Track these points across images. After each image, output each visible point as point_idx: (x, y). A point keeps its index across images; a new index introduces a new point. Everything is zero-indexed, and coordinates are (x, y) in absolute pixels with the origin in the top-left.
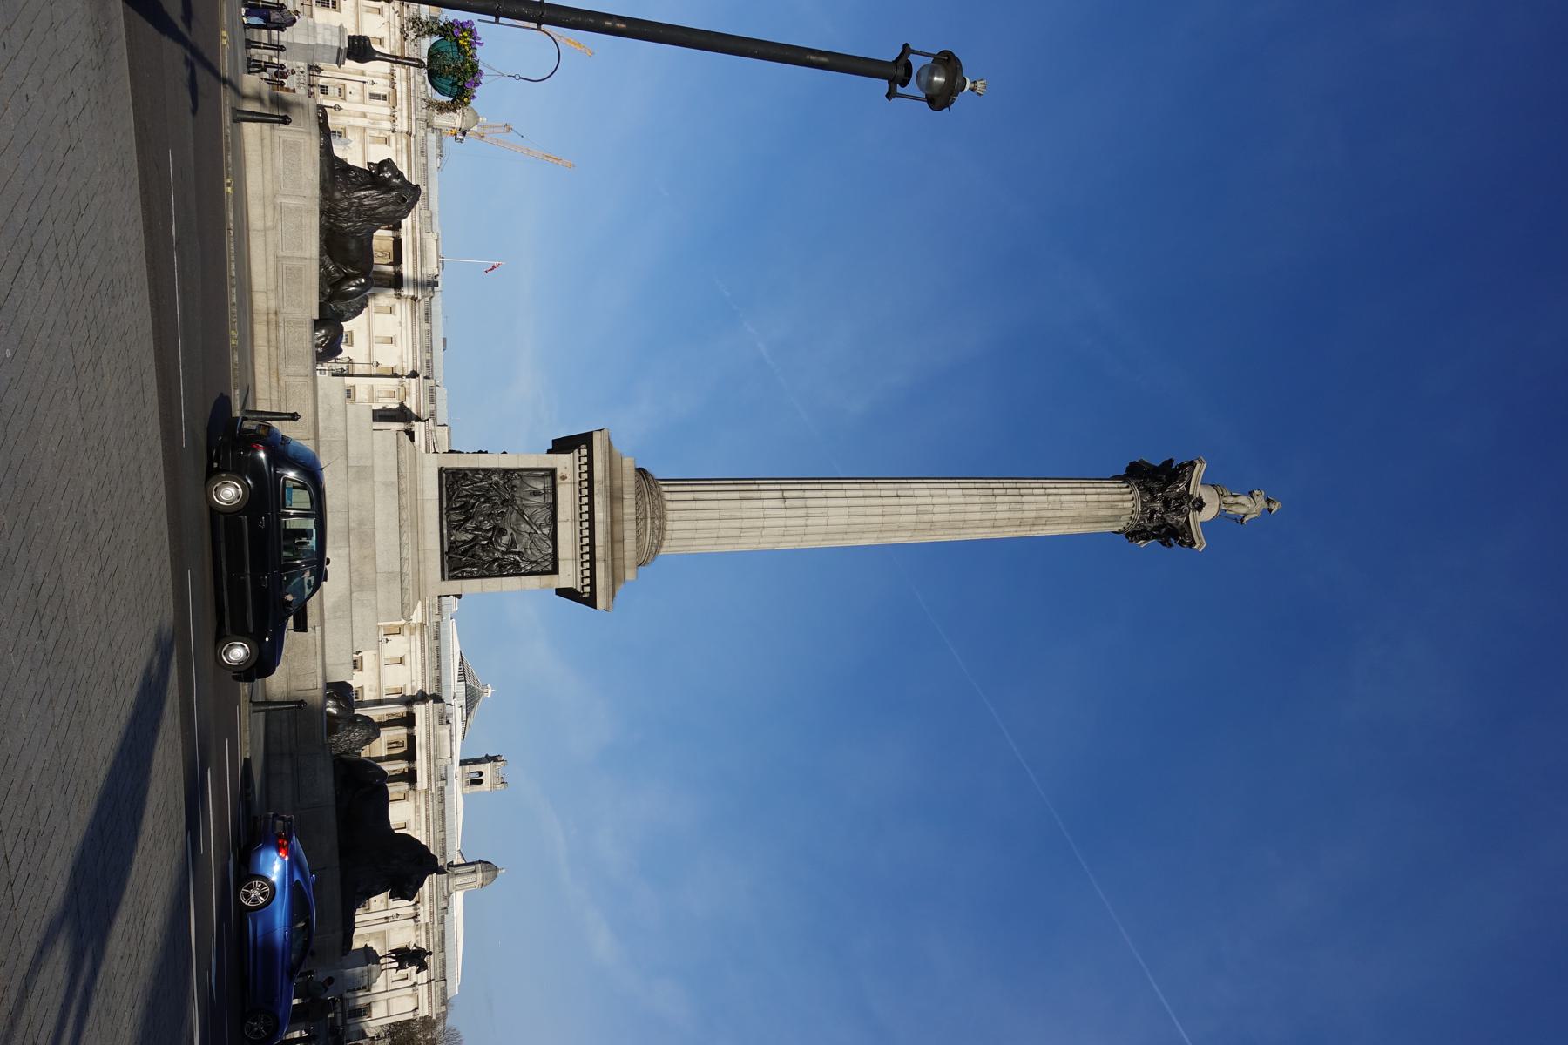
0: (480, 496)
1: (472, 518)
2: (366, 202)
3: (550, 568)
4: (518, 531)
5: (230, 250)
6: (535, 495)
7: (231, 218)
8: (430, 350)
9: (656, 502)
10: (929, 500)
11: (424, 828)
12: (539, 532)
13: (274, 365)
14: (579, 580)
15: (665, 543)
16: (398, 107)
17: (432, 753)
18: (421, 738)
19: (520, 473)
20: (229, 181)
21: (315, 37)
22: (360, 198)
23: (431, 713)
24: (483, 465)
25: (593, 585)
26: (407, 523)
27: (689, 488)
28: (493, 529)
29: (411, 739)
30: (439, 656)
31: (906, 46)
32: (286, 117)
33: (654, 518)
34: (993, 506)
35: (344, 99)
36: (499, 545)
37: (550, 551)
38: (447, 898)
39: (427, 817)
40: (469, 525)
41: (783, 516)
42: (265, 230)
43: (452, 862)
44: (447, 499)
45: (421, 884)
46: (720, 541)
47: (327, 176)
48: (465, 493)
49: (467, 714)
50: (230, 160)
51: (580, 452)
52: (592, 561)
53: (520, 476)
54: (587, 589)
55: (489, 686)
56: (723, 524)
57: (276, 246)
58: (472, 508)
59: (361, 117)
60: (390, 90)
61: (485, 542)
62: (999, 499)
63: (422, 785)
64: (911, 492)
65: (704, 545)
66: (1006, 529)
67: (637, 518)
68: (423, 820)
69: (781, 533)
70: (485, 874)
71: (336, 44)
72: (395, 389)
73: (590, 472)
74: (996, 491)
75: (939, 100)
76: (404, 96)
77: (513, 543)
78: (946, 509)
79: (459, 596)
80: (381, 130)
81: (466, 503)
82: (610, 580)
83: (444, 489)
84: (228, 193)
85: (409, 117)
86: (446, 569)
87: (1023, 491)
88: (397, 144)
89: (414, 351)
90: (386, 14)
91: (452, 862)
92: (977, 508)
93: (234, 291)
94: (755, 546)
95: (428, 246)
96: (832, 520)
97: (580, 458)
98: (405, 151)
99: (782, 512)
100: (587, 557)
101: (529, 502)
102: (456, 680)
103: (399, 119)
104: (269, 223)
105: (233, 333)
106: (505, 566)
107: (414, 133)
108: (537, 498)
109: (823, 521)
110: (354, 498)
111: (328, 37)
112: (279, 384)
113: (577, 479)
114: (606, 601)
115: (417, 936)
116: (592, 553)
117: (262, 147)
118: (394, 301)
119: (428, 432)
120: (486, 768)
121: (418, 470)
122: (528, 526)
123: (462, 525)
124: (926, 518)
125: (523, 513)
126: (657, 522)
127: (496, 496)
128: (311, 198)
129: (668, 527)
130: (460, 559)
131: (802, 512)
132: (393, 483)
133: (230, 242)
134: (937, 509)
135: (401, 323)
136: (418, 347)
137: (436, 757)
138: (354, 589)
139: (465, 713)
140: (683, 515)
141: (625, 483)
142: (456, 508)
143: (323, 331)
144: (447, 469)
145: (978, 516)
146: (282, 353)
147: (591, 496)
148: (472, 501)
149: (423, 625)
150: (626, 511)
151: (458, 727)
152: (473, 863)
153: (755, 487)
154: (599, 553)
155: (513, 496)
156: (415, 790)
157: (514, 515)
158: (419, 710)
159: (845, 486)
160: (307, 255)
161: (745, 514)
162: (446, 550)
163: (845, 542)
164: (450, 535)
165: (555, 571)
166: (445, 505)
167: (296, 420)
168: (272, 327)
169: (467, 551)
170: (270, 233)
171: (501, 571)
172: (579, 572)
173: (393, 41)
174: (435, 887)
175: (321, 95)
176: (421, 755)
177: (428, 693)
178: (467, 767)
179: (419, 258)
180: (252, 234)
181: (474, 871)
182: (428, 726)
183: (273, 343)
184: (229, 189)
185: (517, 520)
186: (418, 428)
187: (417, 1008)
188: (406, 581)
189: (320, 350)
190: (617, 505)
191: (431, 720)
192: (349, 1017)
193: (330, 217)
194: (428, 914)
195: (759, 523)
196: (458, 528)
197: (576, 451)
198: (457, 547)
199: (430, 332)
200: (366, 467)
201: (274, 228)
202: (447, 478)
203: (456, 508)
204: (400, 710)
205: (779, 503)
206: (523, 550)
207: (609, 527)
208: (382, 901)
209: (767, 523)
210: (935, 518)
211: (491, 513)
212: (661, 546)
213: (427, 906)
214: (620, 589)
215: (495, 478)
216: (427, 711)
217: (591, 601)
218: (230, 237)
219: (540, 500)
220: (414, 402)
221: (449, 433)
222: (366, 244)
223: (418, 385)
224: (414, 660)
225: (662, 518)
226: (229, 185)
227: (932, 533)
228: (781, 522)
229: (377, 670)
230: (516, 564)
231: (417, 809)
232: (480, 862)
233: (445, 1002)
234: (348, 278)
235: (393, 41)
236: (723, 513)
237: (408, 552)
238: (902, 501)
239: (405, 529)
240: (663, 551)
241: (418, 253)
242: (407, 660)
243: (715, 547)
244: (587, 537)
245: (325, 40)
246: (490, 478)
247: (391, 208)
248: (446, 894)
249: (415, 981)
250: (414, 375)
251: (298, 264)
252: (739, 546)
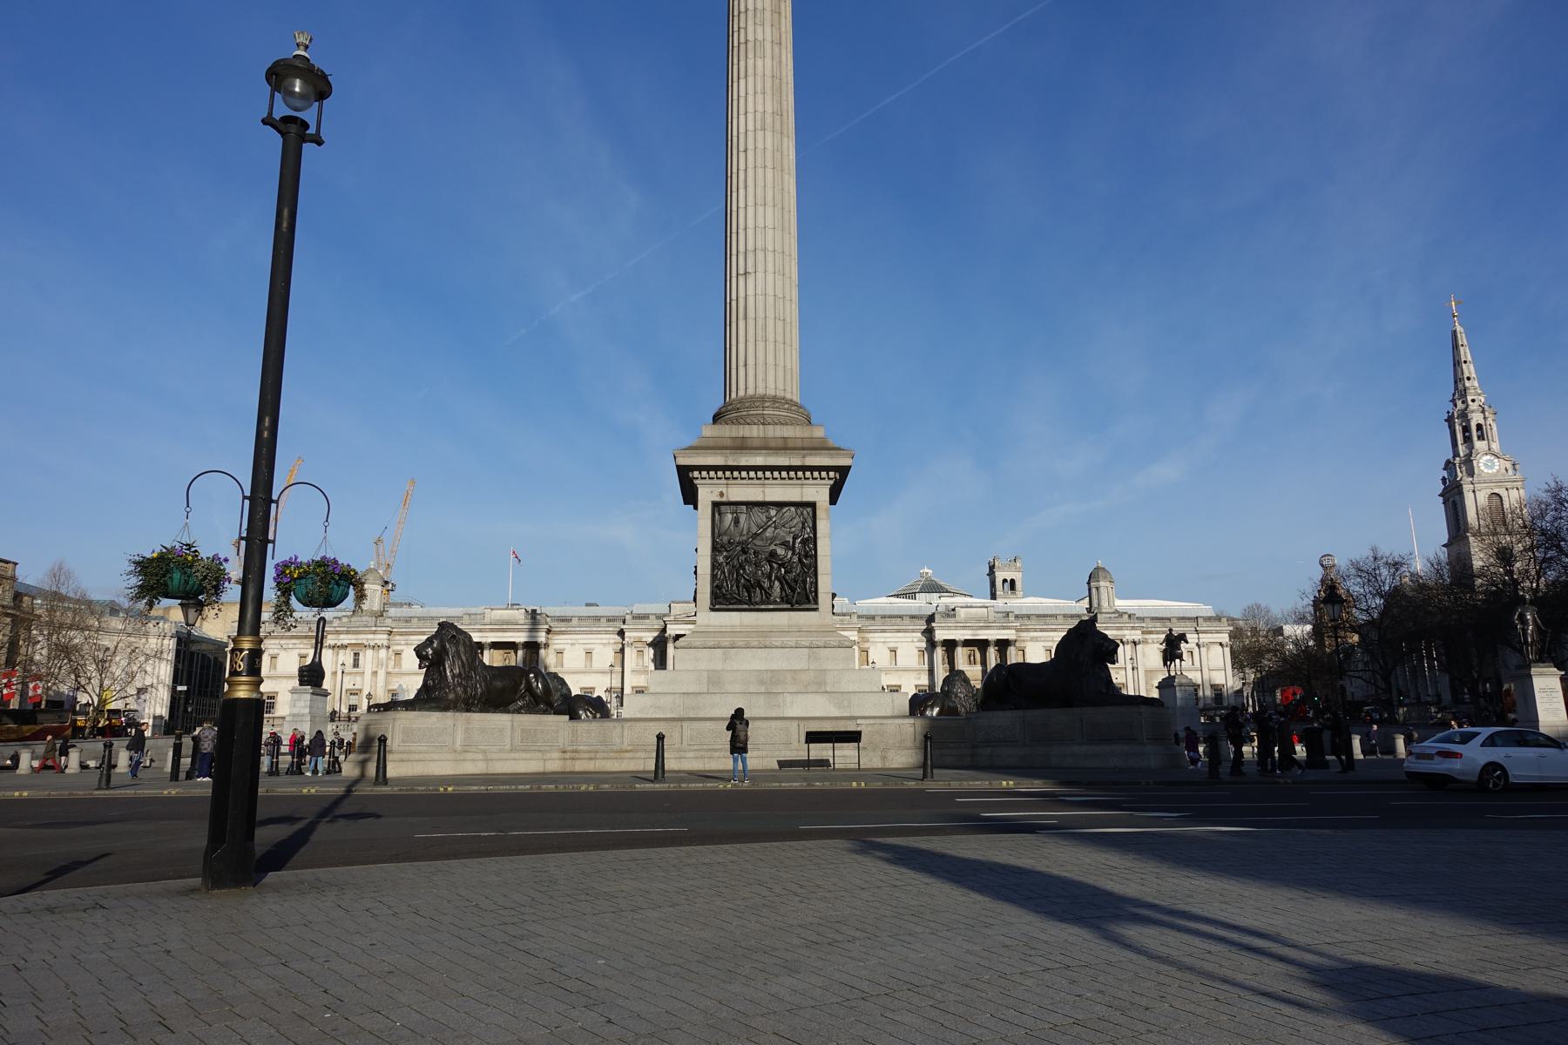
0: (738, 574)
1: (759, 582)
2: (457, 671)
3: (809, 509)
4: (773, 539)
5: (506, 789)
6: (738, 522)
7: (475, 788)
8: (597, 619)
9: (747, 405)
10: (750, 116)
11: (1052, 634)
12: (774, 519)
13: (612, 755)
14: (823, 482)
15: (788, 396)
16: (364, 642)
17: (982, 625)
18: (967, 635)
19: (716, 535)
20: (442, 789)
21: (303, 715)
22: (454, 676)
23: (943, 625)
24: (708, 571)
25: (828, 469)
26: (763, 641)
27: (734, 371)
28: (770, 562)
29: (967, 643)
30: (890, 617)
31: (264, 122)
32: (379, 739)
33: (763, 407)
34: (758, 44)
35: (360, 690)
36: (786, 557)
37: (793, 509)
38: (1121, 614)
39: (1042, 630)
40: (766, 585)
41: (763, 189)
42: (486, 760)
43: (1087, 609)
44: (741, 604)
45: (1106, 635)
46: (788, 341)
47: (433, 705)
48: (735, 588)
49: (947, 592)
50: (423, 788)
51: (697, 478)
52: (804, 468)
53: (719, 536)
54: (832, 474)
55: (921, 571)
56: (771, 337)
57: (501, 751)
58: (749, 581)
59: (376, 676)
60: (349, 649)
61: (783, 570)
62: (750, 37)
64: (742, 136)
65: (792, 358)
66: (783, 29)
67: (763, 424)
69: (781, 277)
70: (1101, 578)
71: (308, 697)
72: (635, 651)
73: (716, 468)
74: (742, 40)
75: (320, 88)
77: (785, 544)
78: (760, 96)
79: (834, 595)
80: (388, 659)
81: (744, 586)
82: (823, 452)
83: (731, 607)
84: (453, 790)
85: (374, 633)
86: (808, 606)
87: (742, 9)
88: (400, 644)
89: (599, 632)
90: (276, 651)
91: (1087, 609)
92: (759, 62)
93: (544, 786)
94: (793, 306)
95: (498, 618)
96: (769, 223)
97: (702, 478)
98: (406, 637)
99: (760, 275)
100: (800, 474)
101: (745, 528)
102: (914, 601)
103: (375, 642)
104: (480, 756)
105: (583, 788)
106: (806, 553)
107: (389, 629)
108: (741, 520)
109: (770, 233)
110: (738, 688)
111: (302, 703)
112: (631, 751)
113: (723, 481)
114: (845, 456)
116: (796, 469)
117: (409, 761)
118: (551, 650)
119: (676, 621)
120: (1000, 576)
121: (712, 630)
122: (769, 530)
123: (765, 591)
124: (769, 119)
125: (755, 534)
126: (767, 404)
127: (738, 559)
128: (455, 720)
129: (773, 393)
130: (798, 593)
131: (760, 255)
132: (724, 653)
133: (499, 789)
134: (760, 108)
135: (572, 644)
136: (594, 629)
137: (985, 622)
138: (824, 690)
139: (946, 594)
140: (761, 377)
141: (727, 435)
142: (750, 596)
143: (581, 712)
144: (712, 604)
145: (768, 61)
146: (602, 748)
147: (740, 468)
148: (742, 581)
149: (860, 630)
150: (755, 434)
151: (959, 600)
152: (1090, 590)
153: (734, 304)
154: (796, 462)
155: (739, 543)
156: (1016, 641)
157: (758, 542)
158: (940, 635)
159: (734, 208)
160: (509, 724)
161: (761, 314)
162: (789, 606)
163: (792, 210)
164: (775, 602)
165: (813, 505)
166: (746, 606)
167: (664, 736)
168: (577, 755)
169: (790, 587)
170: (490, 756)
171: (812, 555)
172: (815, 482)
173: (302, 646)
174: (1109, 625)
175: (358, 711)
176: (983, 635)
177: (925, 627)
178: (997, 593)
179: (509, 627)
180: (491, 771)
181: (1097, 588)
182: (956, 628)
183: (592, 755)
184: (450, 789)
185: (762, 540)
186: (672, 630)
187: (1221, 644)
188: (817, 643)
189: (598, 715)
190: (749, 443)
191: (950, 625)
192: (1222, 703)
193: (473, 704)
195: (770, 299)
196: (768, 595)
197: (695, 482)
198: (787, 596)
199: (580, 618)
200: (708, 676)
201: (484, 752)
202: (720, 604)
203: (750, 596)
204: (939, 652)
205: (751, 279)
206: (792, 535)
207: (771, 452)
208: (1118, 673)
209: (770, 292)
210: (769, 109)
211: (755, 564)
212: (791, 401)
213: (1126, 632)
214: (832, 442)
215: (721, 559)
216: (943, 628)
217: (844, 471)
218: (494, 789)
219: (743, 518)
220: (648, 634)
221: (678, 603)
222: (497, 672)
223: (631, 630)
224: (892, 638)
225: (763, 399)
226: (446, 789)
227: (785, 114)
228: (770, 277)
229: (900, 673)
230: (804, 542)
232: (1089, 583)
233: (1218, 619)
234: (529, 688)
236: (759, 337)
237: (790, 640)
238: (751, 146)
239: (768, 643)
240: (796, 399)
241: (505, 627)
242: (892, 645)
243: (794, 347)
244: (780, 474)
245: (306, 706)
246: (720, 564)
247: (461, 649)
248: (1117, 615)
249: (1195, 645)
250: (621, 633)
251: (518, 733)
252: (794, 322)
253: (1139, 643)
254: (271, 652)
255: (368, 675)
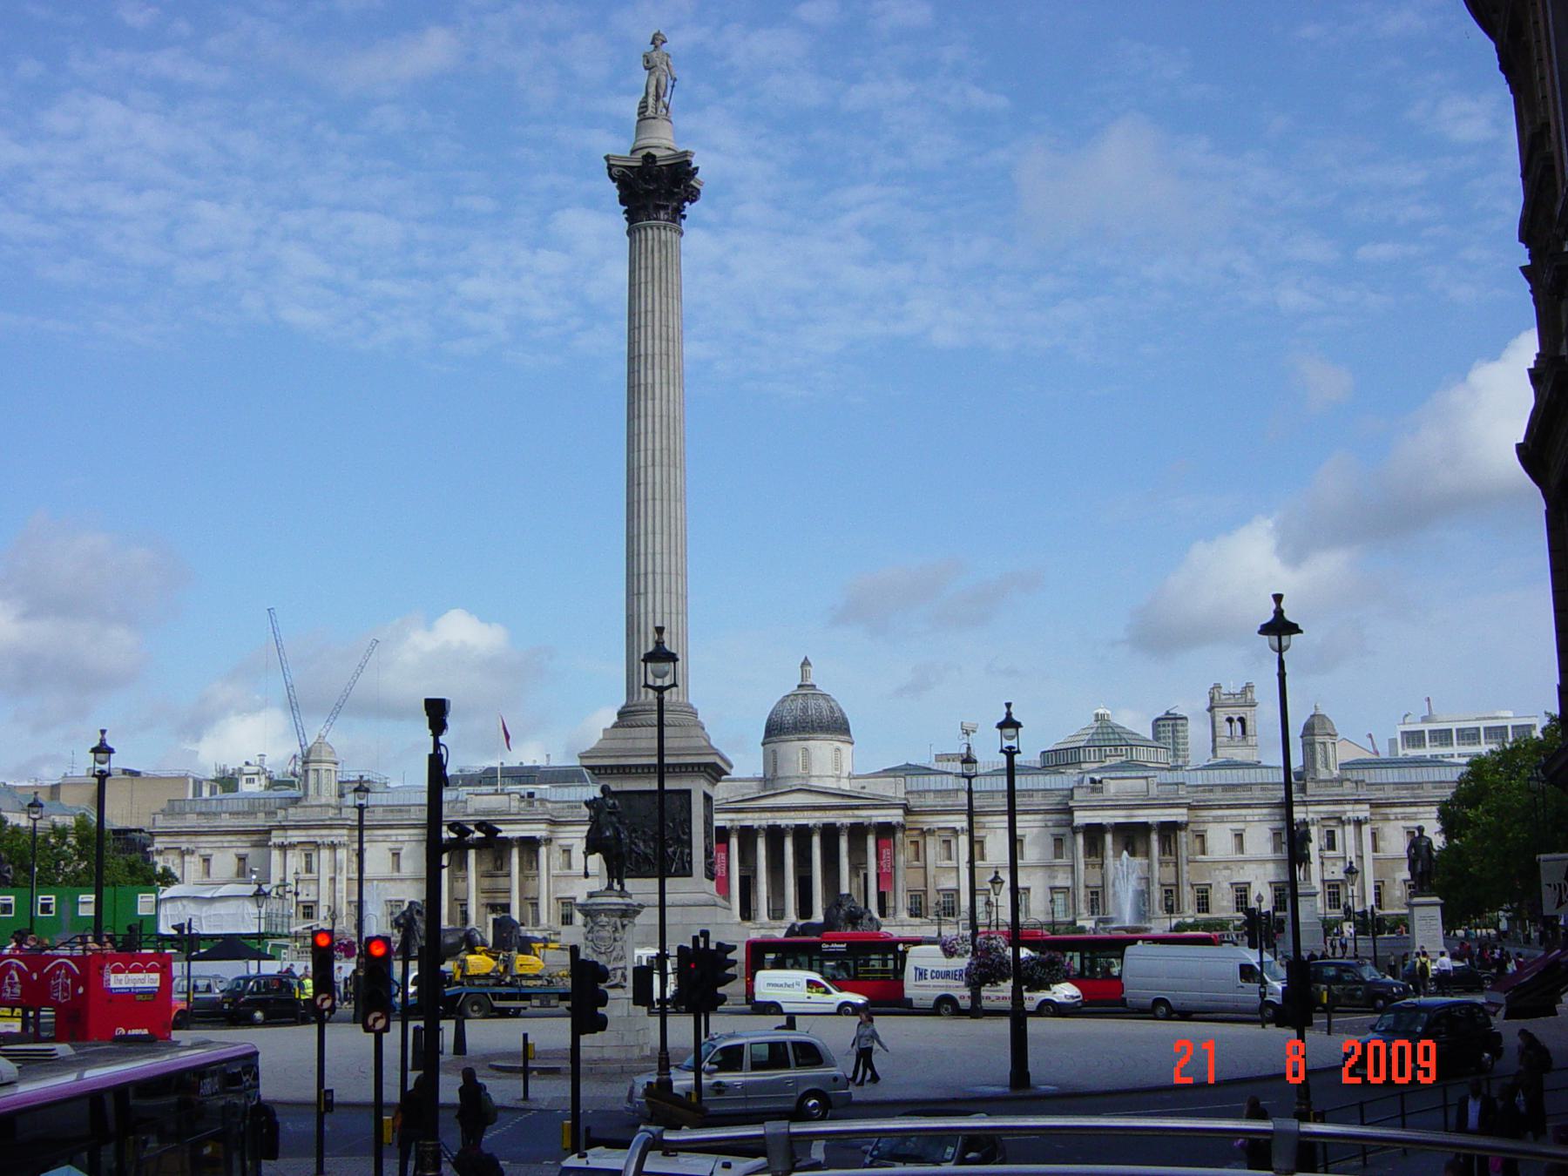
11: (1244, 812)
16: (319, 840)
18: (1119, 817)
29: (1119, 829)
39: (1229, 807)
63: (1182, 815)
68: (1234, 812)
76: (304, 832)
90: (208, 851)
115: (1397, 819)
118: (555, 846)
156: (1187, 824)
158: (1081, 818)
165: (688, 792)
173: (239, 844)
176: (1142, 816)
179: (498, 818)
182: (1103, 808)
194: (1358, 807)
208: (1335, 865)
231: (1220, 820)
235: (239, 844)
253: (1366, 823)
254: (203, 852)
255: (325, 883)
